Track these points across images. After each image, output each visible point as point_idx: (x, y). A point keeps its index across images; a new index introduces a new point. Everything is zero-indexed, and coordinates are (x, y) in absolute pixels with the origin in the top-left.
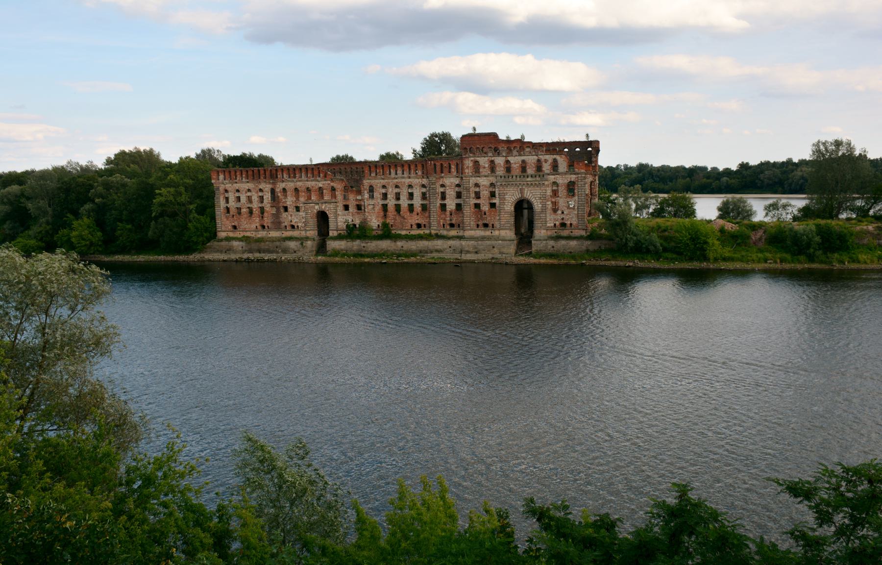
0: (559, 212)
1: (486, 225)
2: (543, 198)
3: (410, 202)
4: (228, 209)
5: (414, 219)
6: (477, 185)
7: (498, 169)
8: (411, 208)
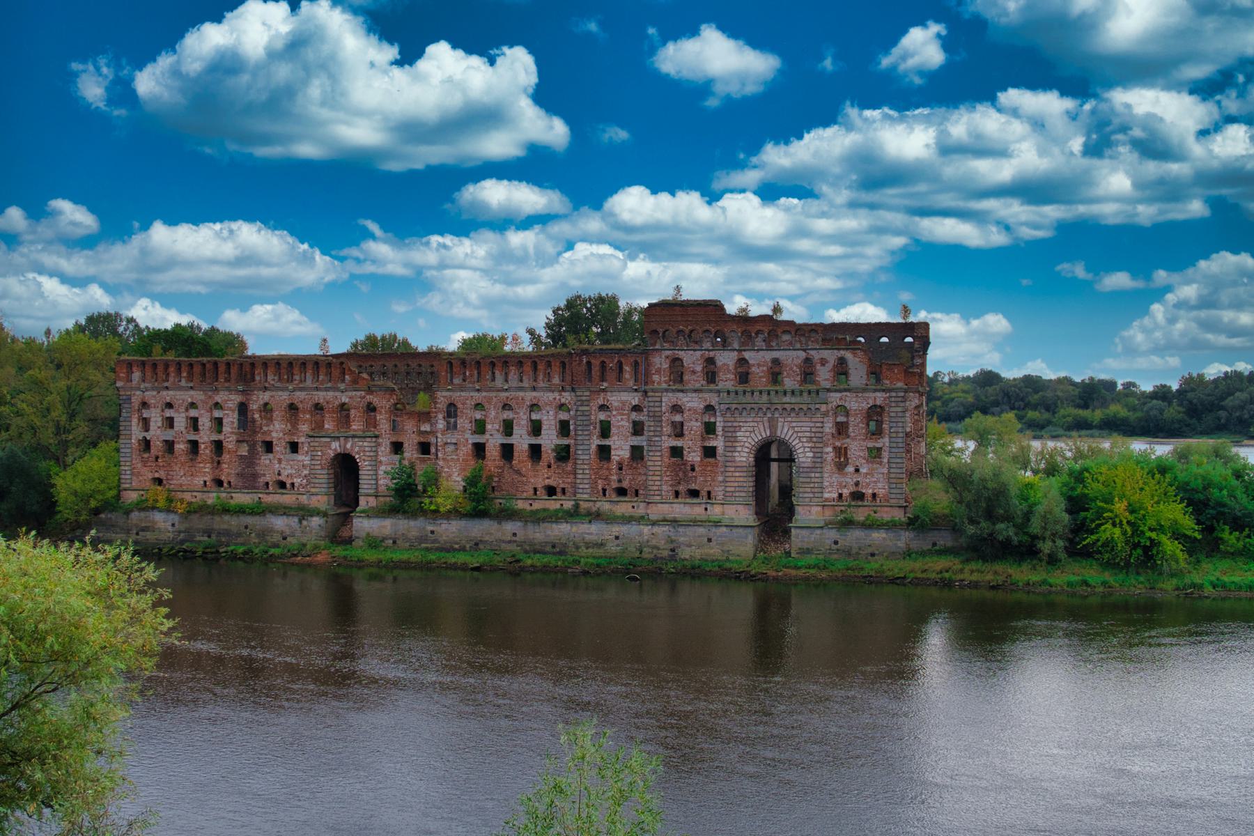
0: (850, 469)
1: (694, 494)
2: (817, 441)
3: (534, 441)
4: (146, 444)
5: (542, 477)
6: (677, 409)
7: (721, 376)
8: (535, 451)
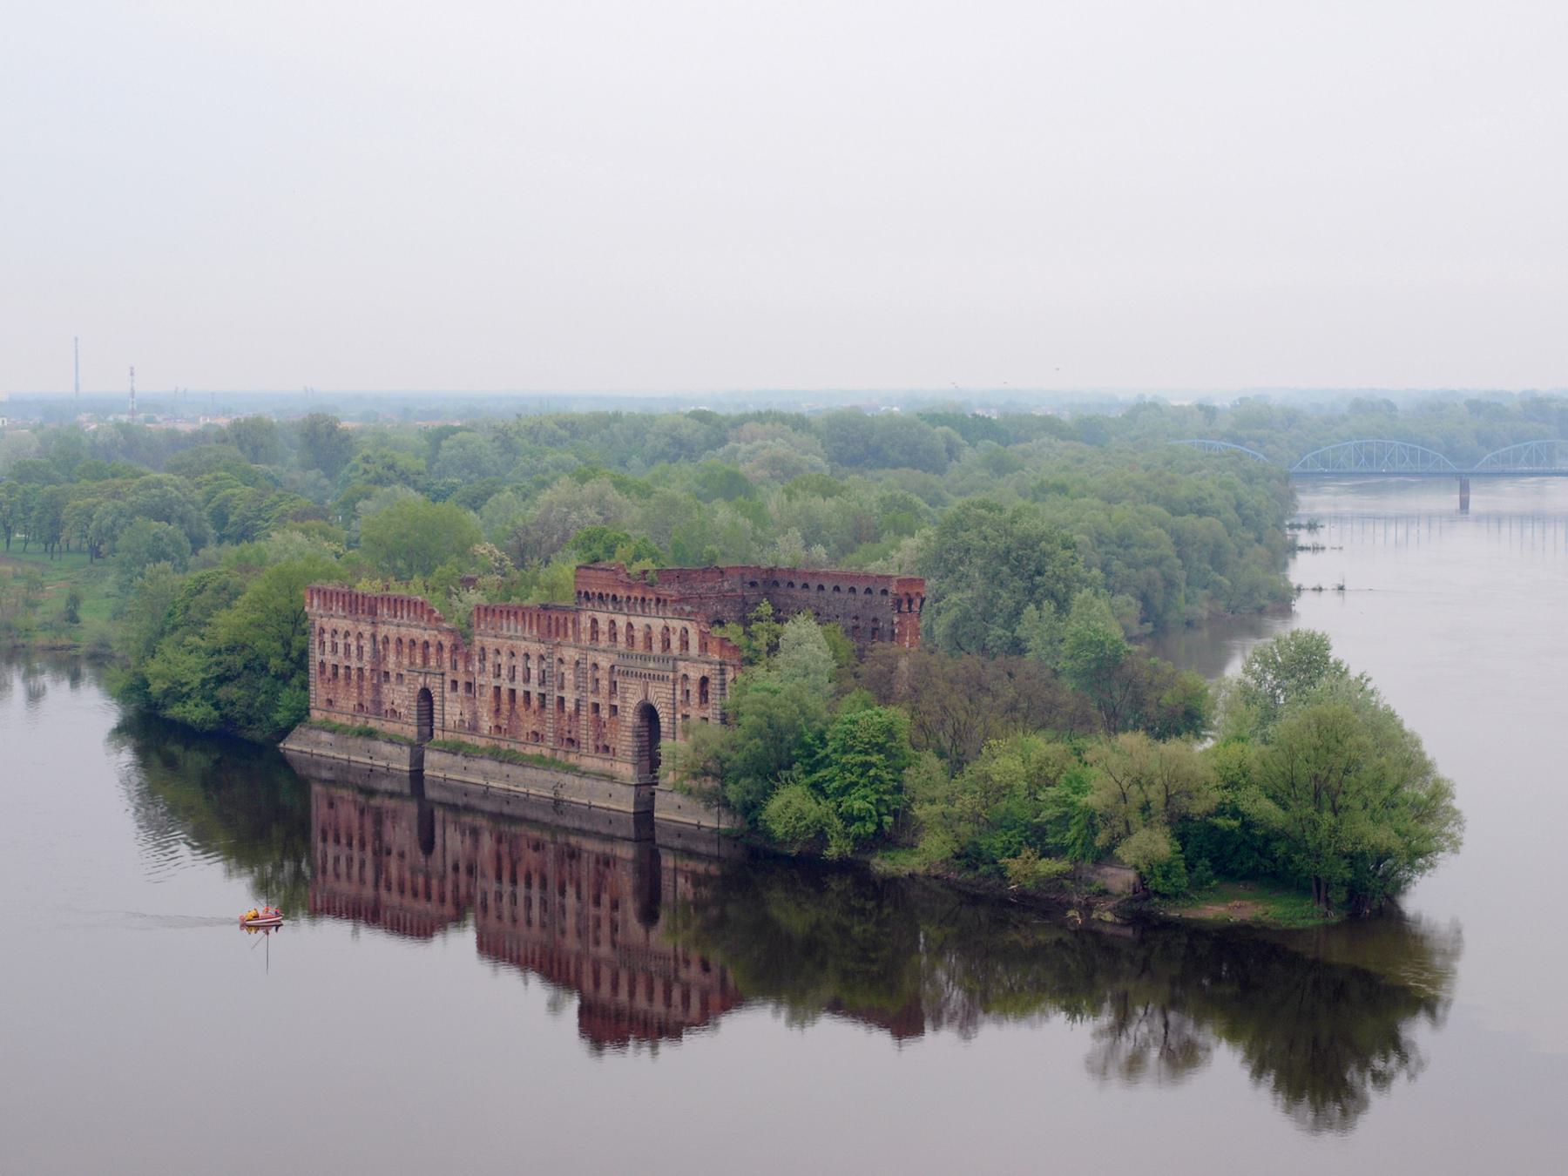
5: (529, 724)
